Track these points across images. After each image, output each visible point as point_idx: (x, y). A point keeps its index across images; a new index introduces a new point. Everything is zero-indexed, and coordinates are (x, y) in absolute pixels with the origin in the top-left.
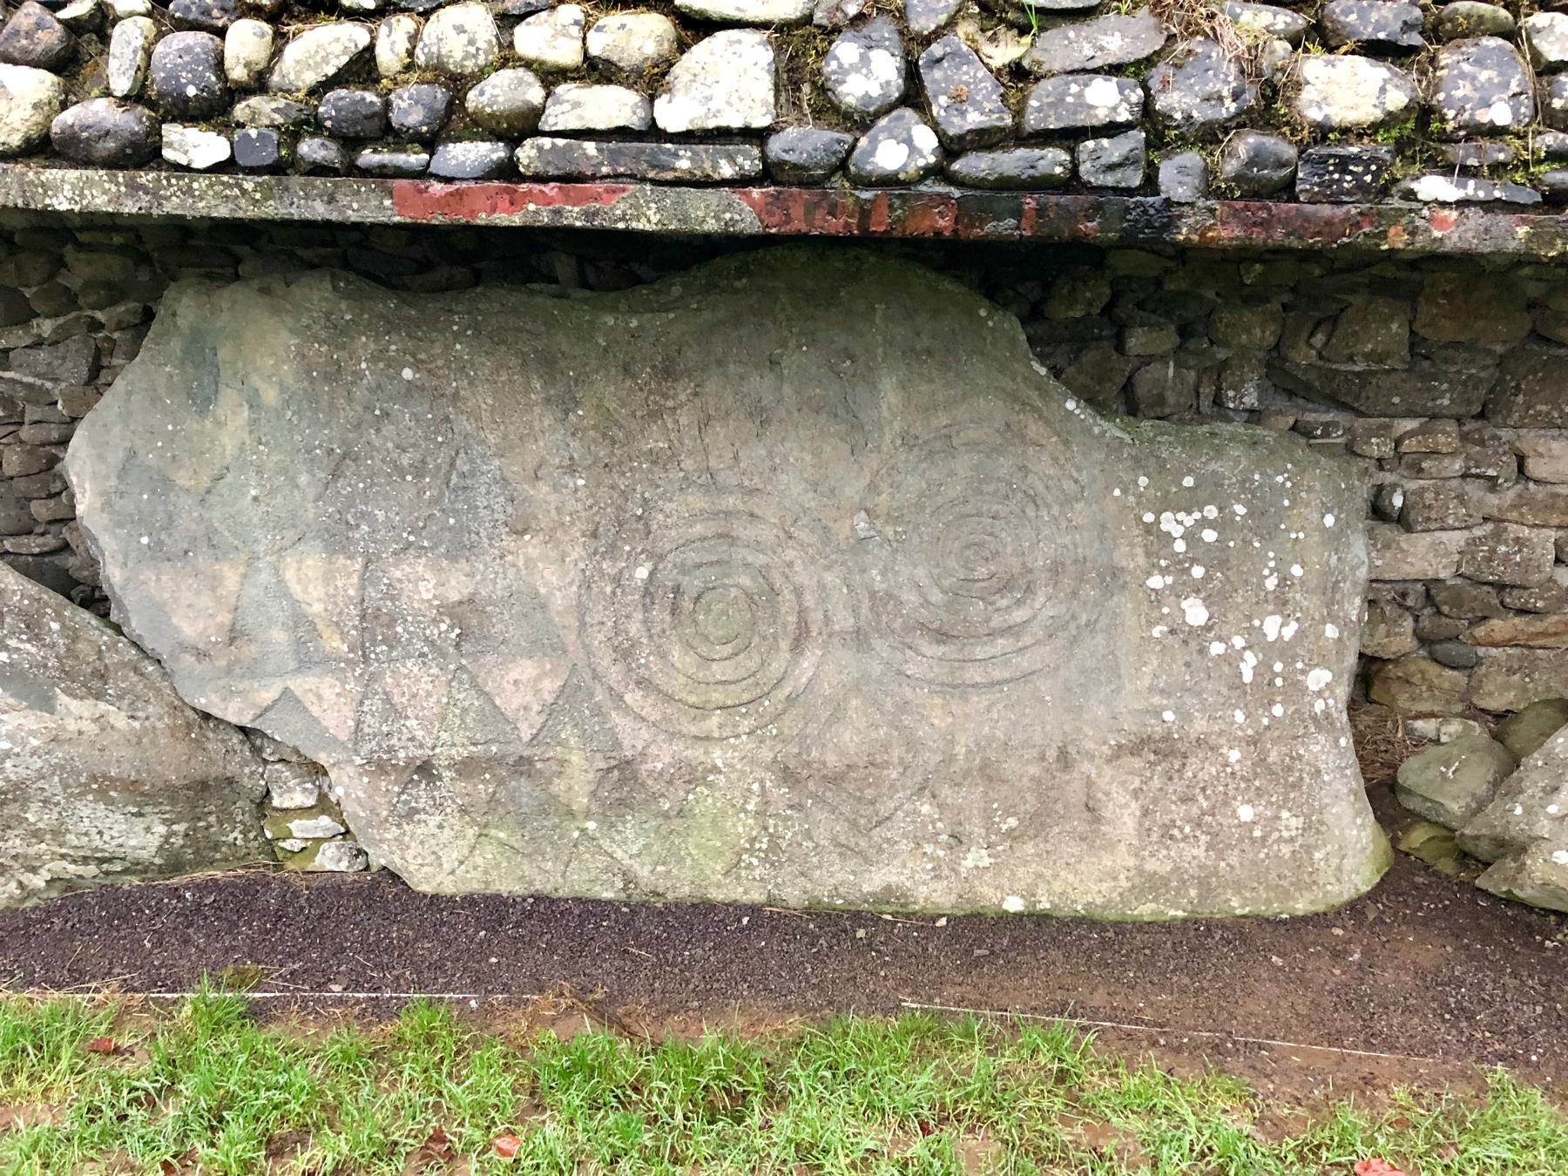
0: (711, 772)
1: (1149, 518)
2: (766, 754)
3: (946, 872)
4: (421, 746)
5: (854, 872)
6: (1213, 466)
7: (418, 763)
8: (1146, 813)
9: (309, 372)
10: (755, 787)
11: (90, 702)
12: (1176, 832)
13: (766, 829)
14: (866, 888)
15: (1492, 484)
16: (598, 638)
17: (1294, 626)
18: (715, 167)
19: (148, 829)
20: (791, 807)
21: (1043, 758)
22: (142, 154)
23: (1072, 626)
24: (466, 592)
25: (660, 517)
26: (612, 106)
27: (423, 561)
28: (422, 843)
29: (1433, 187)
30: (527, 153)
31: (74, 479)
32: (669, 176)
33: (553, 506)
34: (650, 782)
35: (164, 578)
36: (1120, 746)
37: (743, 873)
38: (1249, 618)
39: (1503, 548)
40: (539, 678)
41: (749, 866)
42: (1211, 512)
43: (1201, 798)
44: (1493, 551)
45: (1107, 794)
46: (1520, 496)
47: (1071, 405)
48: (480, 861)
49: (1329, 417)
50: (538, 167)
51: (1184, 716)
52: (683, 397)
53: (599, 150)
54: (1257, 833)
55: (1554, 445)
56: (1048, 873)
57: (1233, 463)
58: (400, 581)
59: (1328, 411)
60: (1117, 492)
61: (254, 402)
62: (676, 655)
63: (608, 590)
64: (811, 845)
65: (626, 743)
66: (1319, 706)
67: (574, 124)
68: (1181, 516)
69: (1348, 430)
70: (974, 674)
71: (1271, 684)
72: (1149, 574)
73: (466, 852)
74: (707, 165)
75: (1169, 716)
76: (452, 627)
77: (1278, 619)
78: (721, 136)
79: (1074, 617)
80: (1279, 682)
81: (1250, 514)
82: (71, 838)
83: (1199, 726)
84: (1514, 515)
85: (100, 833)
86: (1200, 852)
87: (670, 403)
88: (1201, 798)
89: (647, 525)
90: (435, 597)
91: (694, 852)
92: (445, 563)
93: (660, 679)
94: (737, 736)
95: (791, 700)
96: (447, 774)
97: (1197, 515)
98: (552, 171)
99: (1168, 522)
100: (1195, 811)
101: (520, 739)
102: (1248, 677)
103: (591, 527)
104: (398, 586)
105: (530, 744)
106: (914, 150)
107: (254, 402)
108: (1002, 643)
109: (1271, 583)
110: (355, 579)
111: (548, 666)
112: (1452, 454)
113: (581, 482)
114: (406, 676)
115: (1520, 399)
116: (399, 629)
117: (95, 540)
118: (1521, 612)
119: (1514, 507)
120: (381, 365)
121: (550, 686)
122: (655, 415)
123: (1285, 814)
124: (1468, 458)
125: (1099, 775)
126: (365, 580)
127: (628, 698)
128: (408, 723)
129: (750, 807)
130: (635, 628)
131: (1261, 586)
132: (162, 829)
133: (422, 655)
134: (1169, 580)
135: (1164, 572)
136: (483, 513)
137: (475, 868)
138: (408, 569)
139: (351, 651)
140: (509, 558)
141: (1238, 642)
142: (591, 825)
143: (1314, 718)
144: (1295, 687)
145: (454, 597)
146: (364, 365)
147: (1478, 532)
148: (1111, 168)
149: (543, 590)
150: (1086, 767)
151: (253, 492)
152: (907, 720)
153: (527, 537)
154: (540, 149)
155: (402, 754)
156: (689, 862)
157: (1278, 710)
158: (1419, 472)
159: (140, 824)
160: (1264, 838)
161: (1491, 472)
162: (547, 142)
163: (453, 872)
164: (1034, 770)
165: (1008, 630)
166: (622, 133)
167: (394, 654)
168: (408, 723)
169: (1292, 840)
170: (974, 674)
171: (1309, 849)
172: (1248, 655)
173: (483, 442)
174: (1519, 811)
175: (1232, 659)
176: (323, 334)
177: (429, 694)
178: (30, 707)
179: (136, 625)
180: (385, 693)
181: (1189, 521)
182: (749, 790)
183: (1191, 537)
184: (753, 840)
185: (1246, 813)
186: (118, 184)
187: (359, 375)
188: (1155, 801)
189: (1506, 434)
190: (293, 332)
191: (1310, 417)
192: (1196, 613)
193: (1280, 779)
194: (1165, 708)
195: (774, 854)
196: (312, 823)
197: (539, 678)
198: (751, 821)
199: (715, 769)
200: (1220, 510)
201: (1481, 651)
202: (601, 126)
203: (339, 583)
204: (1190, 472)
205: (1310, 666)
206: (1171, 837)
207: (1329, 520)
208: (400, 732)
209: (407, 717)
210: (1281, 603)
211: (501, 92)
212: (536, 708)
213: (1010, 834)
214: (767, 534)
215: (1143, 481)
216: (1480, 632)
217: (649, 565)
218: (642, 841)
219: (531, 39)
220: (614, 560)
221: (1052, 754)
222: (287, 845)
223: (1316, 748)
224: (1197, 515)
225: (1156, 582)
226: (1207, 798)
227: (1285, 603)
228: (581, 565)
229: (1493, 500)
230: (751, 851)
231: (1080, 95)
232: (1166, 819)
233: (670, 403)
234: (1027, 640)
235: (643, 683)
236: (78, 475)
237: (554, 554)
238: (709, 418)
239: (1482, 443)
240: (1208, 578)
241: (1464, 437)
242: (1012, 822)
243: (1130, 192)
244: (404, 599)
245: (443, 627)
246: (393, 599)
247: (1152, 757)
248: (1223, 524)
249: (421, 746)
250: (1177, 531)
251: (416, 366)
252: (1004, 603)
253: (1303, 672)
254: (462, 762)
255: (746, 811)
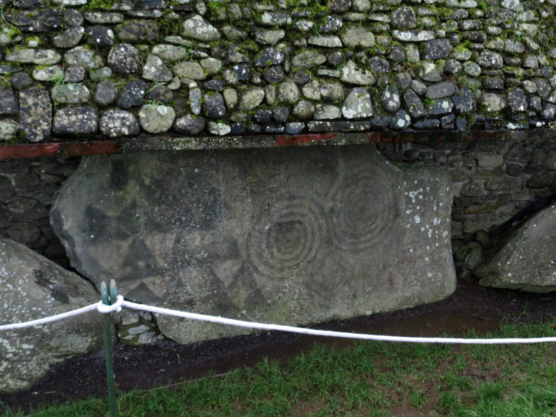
0: (284, 288)
1: (406, 194)
2: (301, 280)
3: (350, 306)
4: (190, 295)
5: (324, 312)
6: (422, 177)
7: (188, 301)
8: (405, 279)
9: (163, 173)
10: (297, 291)
11: (77, 298)
12: (413, 284)
13: (299, 304)
14: (328, 316)
15: (470, 168)
16: (252, 251)
17: (440, 220)
18: (360, 128)
19: (87, 341)
20: (308, 295)
21: (378, 268)
22: (206, 132)
23: (387, 228)
24: (210, 241)
25: (274, 209)
26: (332, 112)
27: (197, 232)
28: (186, 328)
29: (511, 126)
30: (311, 126)
31: (63, 217)
32: (348, 130)
33: (241, 208)
34: (265, 295)
35: (99, 249)
36: (399, 261)
37: (291, 319)
38: (430, 219)
39: (473, 187)
40: (232, 266)
41: (294, 316)
42: (421, 190)
43: (419, 273)
44: (470, 187)
45: (395, 276)
46: (476, 171)
47: (387, 163)
48: (205, 330)
49: (427, 150)
50: (314, 130)
51: (415, 250)
52: (282, 170)
53: (331, 124)
54: (432, 280)
55: (486, 157)
56: (378, 302)
57: (425, 176)
58: (188, 240)
59: (426, 148)
60: (399, 187)
61: (142, 184)
62: (275, 251)
63: (256, 234)
64: (312, 306)
65: (258, 284)
66: (446, 242)
67: (324, 118)
68: (414, 192)
69: (434, 154)
70: (362, 246)
71: (435, 237)
72: (406, 210)
73: (201, 328)
74: (358, 127)
75: (411, 250)
76: (205, 253)
77: (436, 219)
78: (362, 119)
79: (387, 225)
80: (437, 236)
81: (430, 190)
82: (62, 349)
83: (419, 252)
84: (475, 177)
85: (72, 345)
86: (418, 288)
87: (278, 172)
88: (419, 273)
89: (269, 213)
90: (200, 244)
91: (277, 315)
92: (204, 232)
93: (270, 261)
94: (292, 276)
95: (309, 262)
96: (198, 303)
97: (418, 192)
98: (318, 131)
99: (412, 195)
100: (417, 277)
101: (224, 287)
102: (430, 236)
103: (251, 215)
104: (188, 242)
105: (227, 288)
106: (406, 121)
107: (142, 184)
108: (369, 236)
109: (435, 209)
110: (173, 241)
111: (236, 262)
112: (460, 161)
113: (250, 200)
114: (188, 272)
115: (477, 144)
116: (186, 256)
117: (69, 238)
118: (476, 204)
119: (475, 174)
120: (188, 168)
121: (236, 269)
122: (272, 176)
123: (439, 274)
124: (464, 161)
125: (393, 270)
126: (178, 241)
127: (260, 269)
128: (186, 288)
129: (295, 298)
130: (264, 246)
131: (433, 210)
132: (90, 340)
133: (194, 264)
134: (411, 211)
135: (410, 209)
136: (218, 214)
137: (204, 333)
138: (191, 235)
139: (168, 265)
140: (226, 228)
141: (428, 226)
142: (244, 312)
143: (445, 245)
144: (440, 237)
145: (206, 242)
146: (182, 169)
147: (466, 182)
148: (448, 124)
149: (235, 237)
150: (390, 269)
151: (137, 215)
152: (342, 263)
153: (232, 220)
154: (315, 125)
155: (182, 299)
156: (275, 318)
157: (437, 245)
158: (453, 166)
159: (85, 339)
160: (434, 281)
161: (471, 165)
162: (317, 123)
163: (195, 336)
164: (376, 272)
165: (371, 232)
166: (337, 120)
167: (184, 265)
168: (186, 288)
169: (440, 281)
170: (362, 246)
171: (443, 282)
172: (430, 231)
173: (219, 191)
174: (499, 264)
175: (426, 231)
176: (168, 159)
177: (196, 277)
178: (62, 304)
179: (85, 268)
180: (179, 279)
181: (416, 193)
182: (296, 292)
183: (416, 197)
184: (295, 308)
185: (430, 275)
186: (196, 141)
187: (180, 172)
188: (408, 276)
189: (473, 154)
190: (159, 160)
191: (422, 150)
192: (418, 220)
193: (436, 264)
194: (410, 248)
195: (302, 311)
196: (137, 328)
197: (232, 266)
198: (295, 302)
199: (286, 287)
200: (423, 189)
201: (466, 216)
202: (332, 118)
203: (167, 243)
204: (416, 179)
205: (444, 231)
206: (412, 285)
207: (448, 189)
208: (183, 291)
209: (186, 286)
210: (437, 214)
211: (302, 108)
212: (231, 276)
213: (369, 292)
214: (304, 210)
215: (405, 183)
216: (467, 211)
217: (269, 225)
218: (261, 314)
219: (308, 92)
220: (259, 224)
221: (381, 266)
222: (126, 338)
223: (445, 254)
224: (418, 192)
225: (408, 212)
226: (421, 272)
227: (438, 214)
228: (248, 227)
229: (469, 172)
230: (294, 312)
231: (441, 106)
232: (410, 280)
233: (278, 172)
234: (375, 233)
235: (266, 264)
236: (65, 216)
237: (239, 224)
238: (290, 176)
239: (468, 157)
240: (420, 209)
241: (463, 154)
242: (370, 288)
243: (452, 129)
244: (189, 246)
245: (202, 253)
246: (185, 246)
247: (407, 263)
248: (424, 194)
249: (190, 295)
250: (413, 196)
251: (199, 167)
252: (369, 223)
253: (442, 233)
254: (203, 298)
255: (293, 299)
